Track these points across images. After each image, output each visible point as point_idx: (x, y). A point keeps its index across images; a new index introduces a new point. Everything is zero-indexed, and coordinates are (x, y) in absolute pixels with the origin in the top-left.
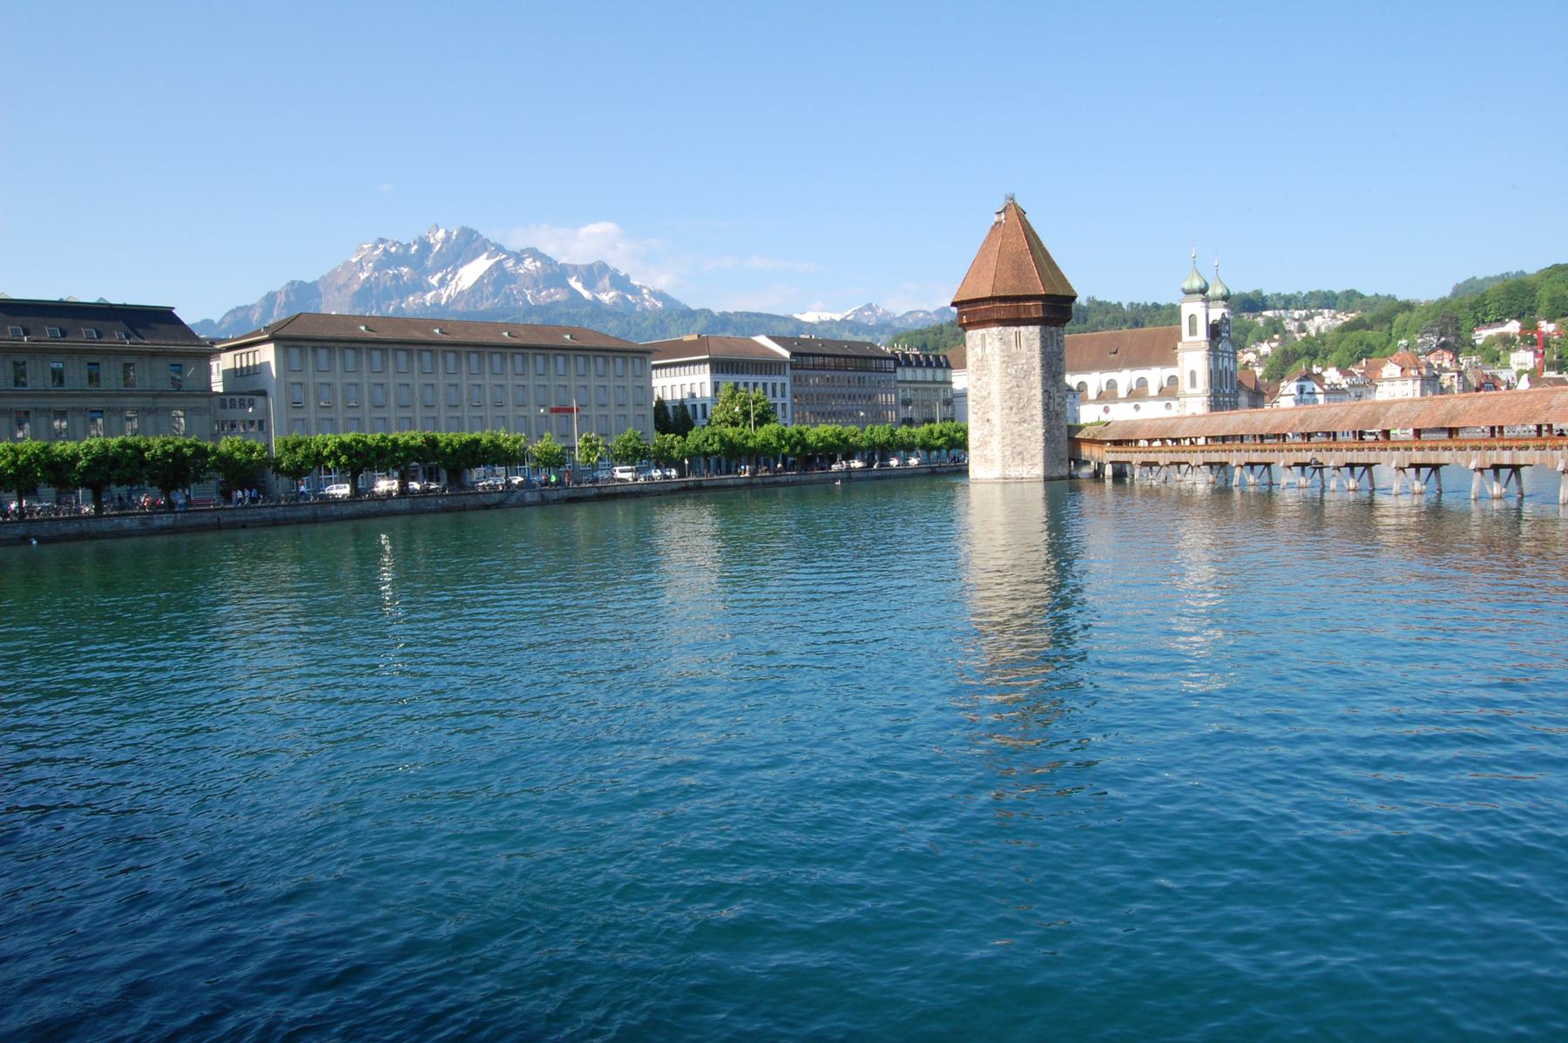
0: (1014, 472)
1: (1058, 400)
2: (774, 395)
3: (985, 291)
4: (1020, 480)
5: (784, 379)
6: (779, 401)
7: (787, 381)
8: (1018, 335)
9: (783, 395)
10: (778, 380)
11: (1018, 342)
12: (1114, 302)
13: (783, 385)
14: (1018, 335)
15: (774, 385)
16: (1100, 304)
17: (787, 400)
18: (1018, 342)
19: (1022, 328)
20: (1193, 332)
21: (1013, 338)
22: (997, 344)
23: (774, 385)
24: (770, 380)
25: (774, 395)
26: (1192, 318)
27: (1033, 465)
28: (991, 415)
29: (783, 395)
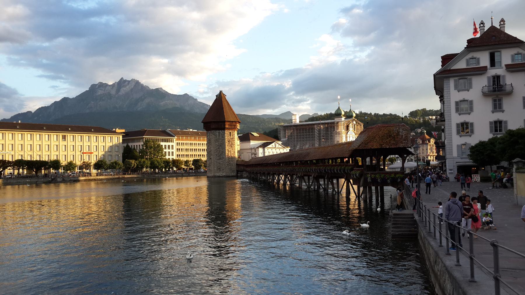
0: (217, 174)
2: (169, 148)
4: (219, 177)
5: (174, 144)
6: (171, 150)
7: (174, 144)
10: (170, 144)
13: (173, 146)
15: (169, 146)
17: (174, 150)
21: (218, 134)
23: (169, 146)
24: (167, 144)
25: (169, 148)
28: (212, 157)
29: (173, 149)
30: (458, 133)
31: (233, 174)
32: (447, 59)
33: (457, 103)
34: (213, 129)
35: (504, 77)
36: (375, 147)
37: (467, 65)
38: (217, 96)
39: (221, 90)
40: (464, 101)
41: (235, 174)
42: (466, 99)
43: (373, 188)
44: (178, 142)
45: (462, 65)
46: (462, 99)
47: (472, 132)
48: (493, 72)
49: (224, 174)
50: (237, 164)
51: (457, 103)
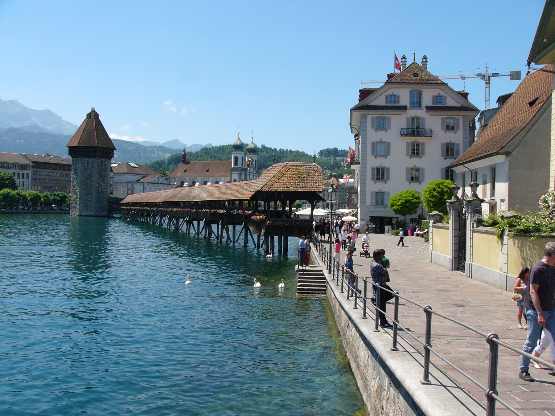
0: (84, 213)
1: (103, 187)
3: (76, 144)
8: (88, 161)
9: (28, 178)
10: (25, 172)
11: (88, 164)
12: (273, 148)
13: (28, 175)
14: (88, 161)
15: (23, 174)
16: (267, 148)
18: (88, 164)
19: (90, 159)
20: (236, 164)
21: (86, 162)
22: (80, 164)
23: (23, 174)
24: (21, 172)
26: (236, 159)
27: (91, 211)
29: (28, 178)
30: (373, 178)
31: (103, 214)
32: (365, 94)
33: (374, 144)
34: (81, 156)
35: (424, 119)
36: (281, 189)
37: (387, 102)
38: (87, 115)
39: (93, 107)
40: (381, 142)
41: (105, 214)
42: (384, 140)
43: (276, 238)
44: (34, 169)
45: (381, 101)
46: (379, 140)
47: (388, 178)
48: (412, 113)
49: (92, 213)
50: (109, 202)
51: (374, 144)
